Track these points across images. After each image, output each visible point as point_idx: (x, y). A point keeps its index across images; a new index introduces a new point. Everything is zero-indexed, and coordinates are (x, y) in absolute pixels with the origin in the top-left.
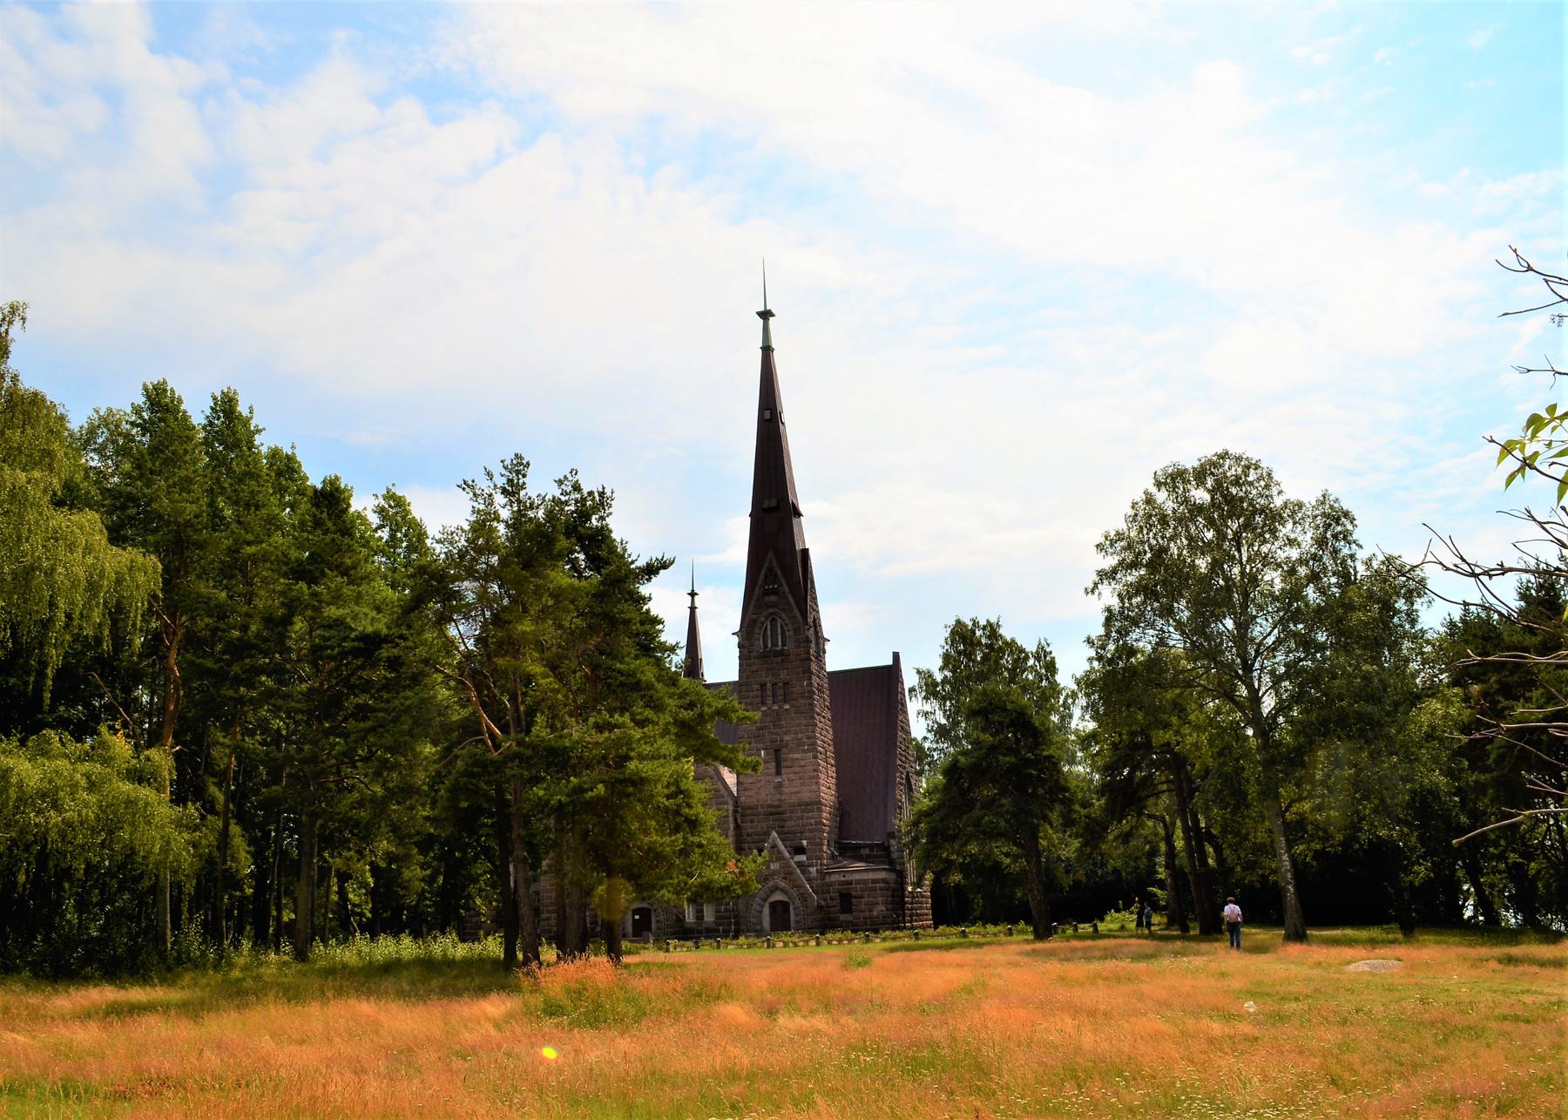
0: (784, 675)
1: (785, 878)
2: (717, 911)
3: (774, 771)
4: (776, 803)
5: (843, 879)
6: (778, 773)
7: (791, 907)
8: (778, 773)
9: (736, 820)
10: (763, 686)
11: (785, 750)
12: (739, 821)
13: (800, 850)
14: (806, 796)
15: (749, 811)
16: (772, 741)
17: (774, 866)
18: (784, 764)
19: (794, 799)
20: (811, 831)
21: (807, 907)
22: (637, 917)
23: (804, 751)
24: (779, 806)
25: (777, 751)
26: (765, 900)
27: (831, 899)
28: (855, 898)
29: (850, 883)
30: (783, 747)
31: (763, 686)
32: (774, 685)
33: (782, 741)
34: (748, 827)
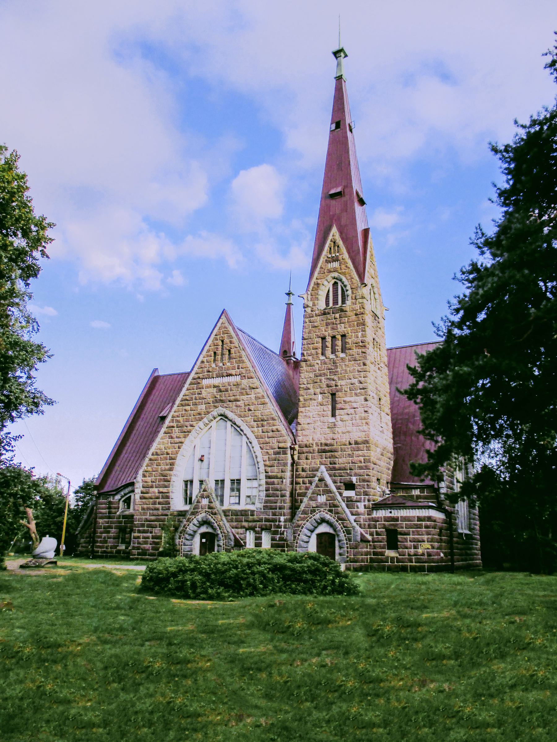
0: (341, 328)
1: (330, 511)
2: (273, 539)
3: (330, 413)
4: (328, 442)
5: (390, 515)
6: (333, 415)
7: (336, 539)
8: (333, 415)
9: (292, 456)
10: (324, 339)
11: (339, 394)
12: (296, 457)
13: (350, 486)
14: (357, 435)
15: (305, 449)
16: (328, 386)
17: (322, 499)
18: (338, 406)
19: (345, 439)
20: (360, 468)
21: (350, 540)
22: (204, 540)
23: (356, 394)
24: (331, 445)
25: (333, 395)
26: (312, 531)
27: (378, 534)
28: (401, 534)
29: (396, 519)
30: (338, 391)
31: (324, 339)
32: (334, 337)
33: (336, 386)
34: (304, 463)
